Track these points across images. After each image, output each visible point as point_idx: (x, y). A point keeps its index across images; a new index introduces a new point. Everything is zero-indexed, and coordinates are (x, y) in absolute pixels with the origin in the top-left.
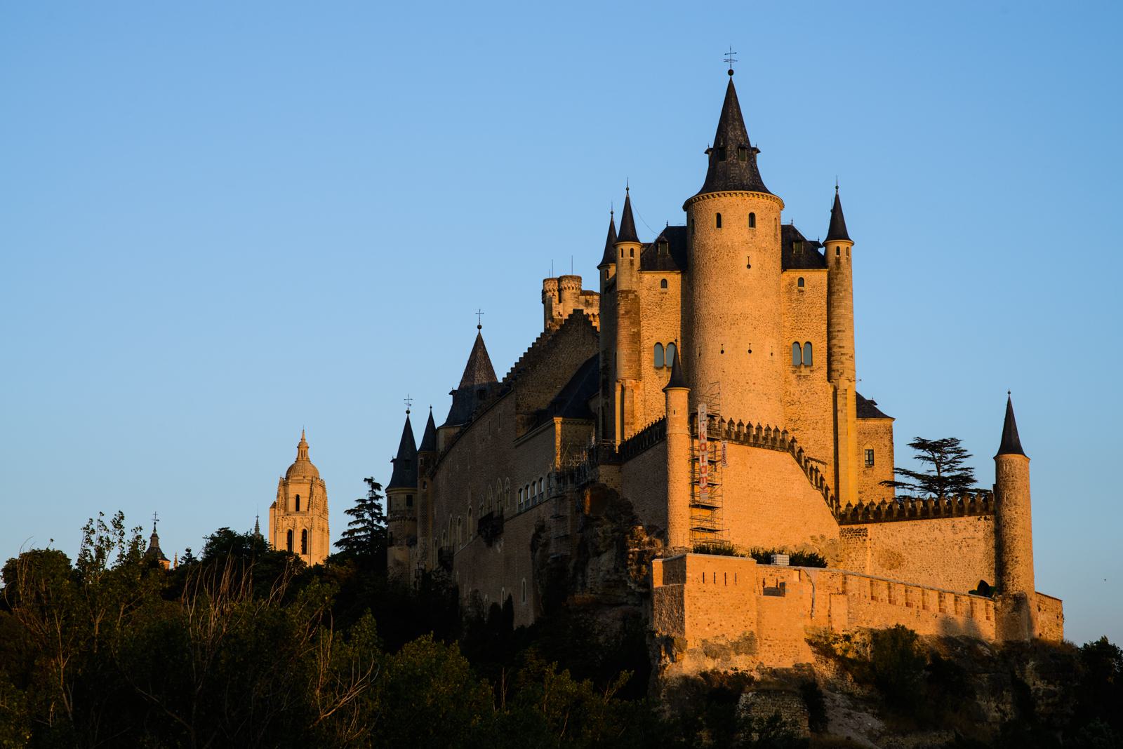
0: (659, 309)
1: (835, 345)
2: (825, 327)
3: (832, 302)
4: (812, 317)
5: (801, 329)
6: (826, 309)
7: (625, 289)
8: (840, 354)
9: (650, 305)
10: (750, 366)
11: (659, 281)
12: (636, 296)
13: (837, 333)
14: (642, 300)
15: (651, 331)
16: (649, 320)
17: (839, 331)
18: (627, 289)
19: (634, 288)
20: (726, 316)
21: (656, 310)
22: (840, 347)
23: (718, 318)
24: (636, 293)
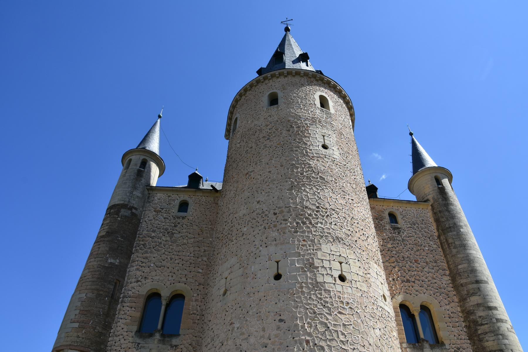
0: (168, 239)
2: (446, 279)
3: (450, 241)
5: (408, 281)
6: (442, 253)
7: (116, 203)
9: (154, 231)
11: (177, 203)
12: (133, 214)
14: (144, 225)
15: (147, 270)
16: (146, 252)
19: (134, 203)
21: (164, 238)
23: (271, 215)
24: (134, 211)
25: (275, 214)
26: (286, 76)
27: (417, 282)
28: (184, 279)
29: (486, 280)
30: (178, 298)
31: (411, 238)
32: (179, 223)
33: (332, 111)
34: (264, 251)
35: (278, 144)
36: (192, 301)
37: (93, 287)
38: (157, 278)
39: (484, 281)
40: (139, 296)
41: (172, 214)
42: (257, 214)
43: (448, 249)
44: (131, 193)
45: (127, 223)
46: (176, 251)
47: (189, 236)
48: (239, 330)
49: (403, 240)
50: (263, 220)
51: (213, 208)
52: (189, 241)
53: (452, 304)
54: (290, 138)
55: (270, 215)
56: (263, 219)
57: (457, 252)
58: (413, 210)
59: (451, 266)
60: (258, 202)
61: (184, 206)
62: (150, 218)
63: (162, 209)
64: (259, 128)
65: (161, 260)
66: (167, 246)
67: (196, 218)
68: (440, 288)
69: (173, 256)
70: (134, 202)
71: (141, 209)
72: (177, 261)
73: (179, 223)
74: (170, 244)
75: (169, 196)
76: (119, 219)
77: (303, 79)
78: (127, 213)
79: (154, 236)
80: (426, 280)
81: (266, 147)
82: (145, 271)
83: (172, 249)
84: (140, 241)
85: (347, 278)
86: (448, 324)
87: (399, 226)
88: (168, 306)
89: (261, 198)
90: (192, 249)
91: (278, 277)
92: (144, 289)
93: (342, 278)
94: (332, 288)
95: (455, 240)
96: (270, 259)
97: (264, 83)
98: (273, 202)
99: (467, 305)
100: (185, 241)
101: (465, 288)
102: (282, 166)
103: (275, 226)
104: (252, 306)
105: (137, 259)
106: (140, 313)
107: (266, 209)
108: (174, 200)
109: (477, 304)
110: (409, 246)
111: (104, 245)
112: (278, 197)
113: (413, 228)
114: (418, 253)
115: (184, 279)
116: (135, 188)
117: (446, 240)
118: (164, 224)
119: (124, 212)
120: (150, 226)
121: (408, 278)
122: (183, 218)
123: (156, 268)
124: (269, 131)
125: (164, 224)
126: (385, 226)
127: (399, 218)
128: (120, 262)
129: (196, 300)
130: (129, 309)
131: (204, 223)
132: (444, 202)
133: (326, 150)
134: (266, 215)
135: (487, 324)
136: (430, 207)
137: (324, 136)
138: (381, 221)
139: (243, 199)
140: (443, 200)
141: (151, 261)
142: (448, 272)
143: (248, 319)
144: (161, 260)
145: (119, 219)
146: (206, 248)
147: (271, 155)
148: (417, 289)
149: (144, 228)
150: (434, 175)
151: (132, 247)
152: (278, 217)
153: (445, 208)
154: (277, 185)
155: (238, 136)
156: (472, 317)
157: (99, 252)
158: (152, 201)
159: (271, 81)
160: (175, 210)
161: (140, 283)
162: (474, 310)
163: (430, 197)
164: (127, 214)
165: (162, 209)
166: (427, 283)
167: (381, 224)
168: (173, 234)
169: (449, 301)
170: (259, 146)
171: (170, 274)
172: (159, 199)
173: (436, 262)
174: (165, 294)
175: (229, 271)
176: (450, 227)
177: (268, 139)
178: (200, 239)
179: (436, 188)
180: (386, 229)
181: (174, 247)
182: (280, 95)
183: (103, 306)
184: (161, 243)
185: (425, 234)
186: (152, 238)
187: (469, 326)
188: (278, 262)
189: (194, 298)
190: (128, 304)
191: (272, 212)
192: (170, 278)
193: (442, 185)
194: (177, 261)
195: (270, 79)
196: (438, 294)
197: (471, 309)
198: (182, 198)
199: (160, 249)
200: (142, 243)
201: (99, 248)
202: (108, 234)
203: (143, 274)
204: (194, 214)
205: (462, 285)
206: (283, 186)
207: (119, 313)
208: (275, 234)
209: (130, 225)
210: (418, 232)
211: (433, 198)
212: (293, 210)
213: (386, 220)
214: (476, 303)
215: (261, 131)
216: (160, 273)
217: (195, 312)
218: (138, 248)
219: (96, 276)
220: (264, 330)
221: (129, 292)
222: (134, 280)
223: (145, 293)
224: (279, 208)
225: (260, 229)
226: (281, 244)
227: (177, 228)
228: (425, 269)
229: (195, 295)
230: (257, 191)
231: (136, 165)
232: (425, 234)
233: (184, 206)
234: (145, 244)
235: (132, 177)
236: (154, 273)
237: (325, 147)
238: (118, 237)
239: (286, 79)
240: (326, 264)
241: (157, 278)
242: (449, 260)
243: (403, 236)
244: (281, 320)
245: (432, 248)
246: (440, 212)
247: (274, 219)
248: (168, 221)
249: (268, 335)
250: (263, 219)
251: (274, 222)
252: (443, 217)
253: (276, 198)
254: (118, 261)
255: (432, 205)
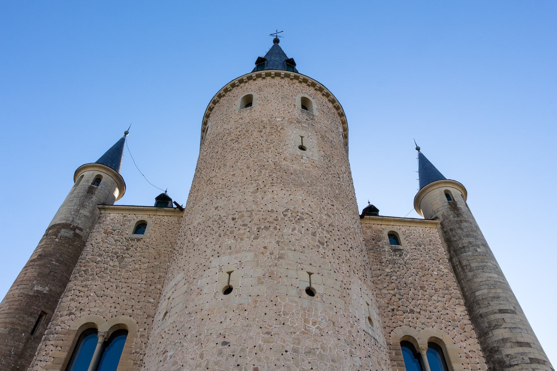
0: (117, 264)
1: (504, 340)
2: (461, 310)
3: (464, 263)
4: (430, 291)
5: (412, 311)
7: (57, 223)
8: (527, 360)
9: (100, 255)
10: (313, 329)
11: (133, 224)
12: (76, 235)
13: (499, 316)
14: (88, 248)
17: (501, 311)
18: (65, 222)
19: (79, 222)
20: (246, 214)
21: (111, 263)
22: (520, 344)
24: (77, 231)
25: (233, 219)
26: (264, 78)
27: (422, 312)
28: (130, 311)
29: (513, 309)
30: (120, 332)
31: (416, 261)
32: (132, 246)
33: (316, 113)
34: (215, 262)
35: (246, 146)
36: (137, 337)
37: (7, 320)
38: (96, 309)
39: (511, 310)
40: (68, 332)
41: (126, 236)
42: (213, 221)
43: (462, 273)
44: (77, 211)
45: (66, 245)
46: (124, 278)
47: (143, 260)
48: (172, 360)
49: (406, 263)
50: (219, 227)
51: (176, 229)
52: (142, 266)
53: (471, 341)
54: (261, 139)
55: (227, 221)
56: (219, 226)
57: (474, 275)
58: (419, 229)
59: (467, 294)
60: (216, 208)
61: (141, 227)
62: (98, 241)
63: (114, 230)
64: (228, 132)
65: (104, 289)
66: (114, 272)
67: (154, 239)
68: (454, 320)
69: (120, 284)
70: (79, 222)
71: (88, 230)
72: (123, 290)
73: (132, 246)
74: (118, 269)
75: (125, 216)
76: (57, 240)
77: (283, 81)
78: (69, 234)
79: (99, 261)
80: (435, 310)
81: (233, 150)
82: (82, 302)
83: (119, 275)
84: (81, 266)
85: (317, 291)
86: (466, 366)
87: (400, 247)
88: (106, 344)
89: (220, 203)
90: (144, 276)
91: (228, 290)
92: (76, 324)
93: (310, 292)
94: (295, 302)
95: (470, 261)
96: (221, 270)
97: (239, 87)
98: (233, 206)
99: (489, 341)
100: (136, 266)
101: (485, 319)
102: (248, 168)
103: (232, 232)
104: (192, 327)
105: (74, 288)
106: (66, 353)
107: (224, 214)
108: (130, 221)
109: (503, 339)
110: (413, 270)
111: (33, 270)
112: (239, 201)
113: (419, 249)
114: (424, 279)
115: (130, 311)
116: (82, 205)
117: (460, 262)
118: (113, 247)
119: (64, 232)
120: (96, 250)
121: (412, 308)
122: (138, 240)
123: (97, 298)
124: (239, 133)
125: (113, 247)
126: (383, 248)
127: (402, 238)
128: (50, 290)
129: (142, 336)
130: (54, 348)
131: (162, 246)
132: (456, 219)
133: (303, 151)
134: (223, 221)
135: (517, 365)
136: (440, 226)
137: (302, 137)
138: (379, 241)
139: (201, 207)
140: (454, 217)
141: (91, 290)
142: (462, 302)
143: (185, 344)
144: (104, 289)
145: (57, 240)
146: (162, 274)
147: (237, 158)
148: (423, 321)
149: (88, 252)
150: (444, 189)
151: (70, 274)
152: (236, 222)
153: (458, 226)
154: (240, 188)
155: (206, 144)
156: (496, 357)
157: (25, 278)
158: (104, 221)
159: (247, 84)
160: (129, 231)
161: (73, 316)
162: (499, 347)
163: (439, 214)
164: (68, 235)
165: (114, 230)
166: (437, 314)
167: (379, 246)
168: (123, 258)
169: (466, 337)
170: (225, 150)
171: (113, 305)
172: (112, 220)
173: (447, 289)
174: (104, 328)
175: (173, 289)
176: (464, 247)
177: (237, 141)
178: (156, 263)
179: (447, 204)
180: (385, 251)
181: (123, 273)
182: (255, 96)
183: (17, 343)
184: (107, 269)
185: (434, 257)
186: (97, 263)
187: (494, 368)
188: (229, 273)
189: (139, 334)
190: (52, 343)
191: (230, 217)
192: (113, 309)
193: (454, 200)
194: (123, 290)
195: (246, 82)
196: (451, 328)
197: (495, 345)
198: (140, 218)
199: (105, 275)
200: (84, 269)
201: (25, 274)
202: (40, 257)
203: (78, 305)
204: (153, 236)
205: (481, 315)
206: (247, 188)
207: (38, 354)
208: (230, 241)
209: (71, 247)
210: (424, 255)
211: (443, 215)
212: (256, 214)
213: (385, 241)
214: (500, 338)
215: (229, 134)
216: (101, 304)
217: (138, 350)
218: (78, 275)
219: (15, 307)
220: (202, 356)
221: (57, 328)
222: (65, 313)
223: (77, 328)
224: (240, 212)
225: (214, 237)
226: (237, 252)
227: (129, 252)
228: (433, 298)
229: (141, 330)
230: (216, 197)
231: (88, 181)
232: (434, 257)
233: (141, 227)
234: (88, 269)
235: (81, 194)
236: (92, 304)
237: (302, 148)
238: (52, 260)
239: (264, 81)
240: (292, 273)
241: (96, 309)
242: (464, 285)
243: (406, 258)
244: (225, 343)
245: (442, 273)
246: (451, 230)
247: (232, 225)
248: (119, 243)
249: (206, 363)
250: (219, 226)
251: (232, 227)
252: (454, 236)
253: (237, 201)
254: (47, 289)
255: (441, 224)
